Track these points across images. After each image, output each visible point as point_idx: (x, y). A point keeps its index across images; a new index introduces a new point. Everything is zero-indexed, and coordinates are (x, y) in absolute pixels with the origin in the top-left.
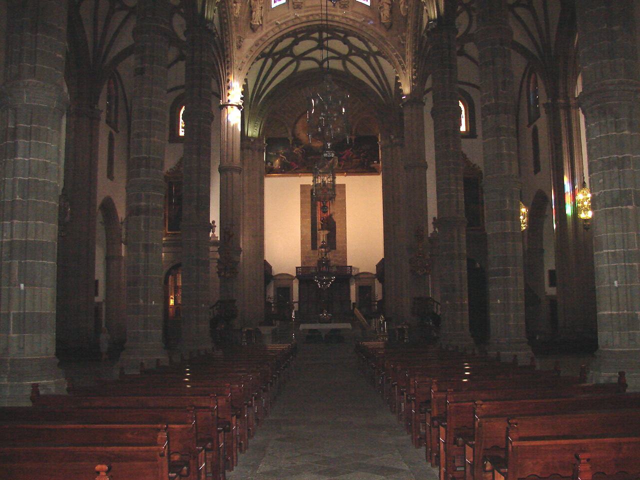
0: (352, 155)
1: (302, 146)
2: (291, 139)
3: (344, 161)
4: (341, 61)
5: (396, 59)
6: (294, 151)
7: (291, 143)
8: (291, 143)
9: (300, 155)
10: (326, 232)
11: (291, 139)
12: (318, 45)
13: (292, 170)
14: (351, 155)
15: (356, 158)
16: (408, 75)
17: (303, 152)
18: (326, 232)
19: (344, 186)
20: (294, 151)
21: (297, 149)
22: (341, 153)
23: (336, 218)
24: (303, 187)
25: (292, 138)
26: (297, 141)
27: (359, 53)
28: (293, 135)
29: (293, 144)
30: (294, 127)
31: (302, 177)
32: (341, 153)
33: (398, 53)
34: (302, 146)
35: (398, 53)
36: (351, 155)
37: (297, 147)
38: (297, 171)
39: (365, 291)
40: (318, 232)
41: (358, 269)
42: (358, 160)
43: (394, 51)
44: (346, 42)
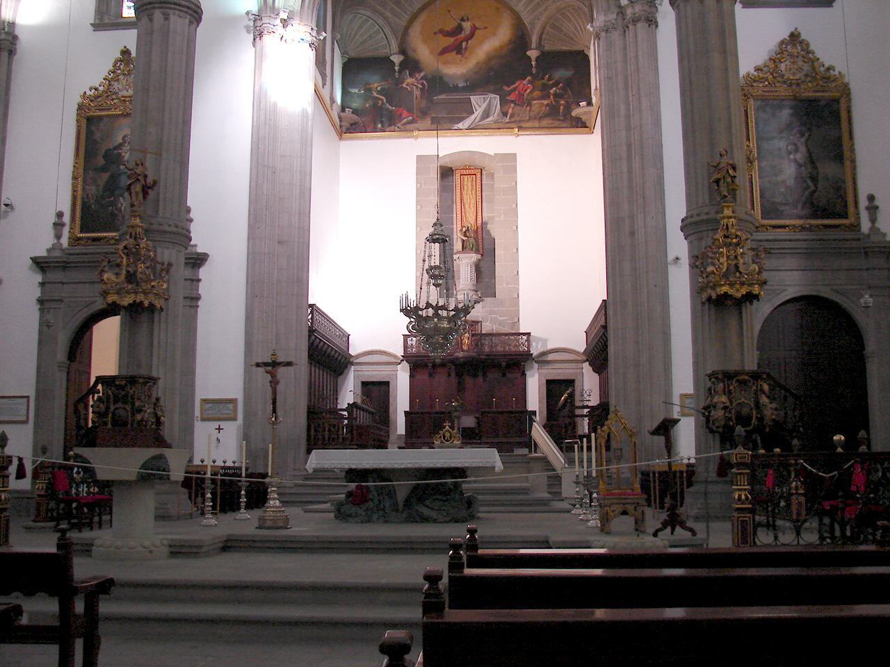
1: (422, 74)
2: (397, 59)
6: (404, 85)
7: (397, 68)
8: (397, 68)
9: (417, 93)
10: (474, 257)
11: (397, 59)
13: (399, 125)
14: (528, 91)
15: (542, 98)
18: (474, 257)
19: (512, 157)
20: (404, 85)
21: (410, 80)
23: (496, 230)
26: (411, 65)
28: (403, 52)
29: (400, 72)
31: (420, 140)
32: (506, 88)
34: (422, 74)
36: (528, 91)
37: (411, 75)
38: (408, 127)
39: (557, 389)
40: (455, 257)
41: (545, 341)
42: (545, 102)
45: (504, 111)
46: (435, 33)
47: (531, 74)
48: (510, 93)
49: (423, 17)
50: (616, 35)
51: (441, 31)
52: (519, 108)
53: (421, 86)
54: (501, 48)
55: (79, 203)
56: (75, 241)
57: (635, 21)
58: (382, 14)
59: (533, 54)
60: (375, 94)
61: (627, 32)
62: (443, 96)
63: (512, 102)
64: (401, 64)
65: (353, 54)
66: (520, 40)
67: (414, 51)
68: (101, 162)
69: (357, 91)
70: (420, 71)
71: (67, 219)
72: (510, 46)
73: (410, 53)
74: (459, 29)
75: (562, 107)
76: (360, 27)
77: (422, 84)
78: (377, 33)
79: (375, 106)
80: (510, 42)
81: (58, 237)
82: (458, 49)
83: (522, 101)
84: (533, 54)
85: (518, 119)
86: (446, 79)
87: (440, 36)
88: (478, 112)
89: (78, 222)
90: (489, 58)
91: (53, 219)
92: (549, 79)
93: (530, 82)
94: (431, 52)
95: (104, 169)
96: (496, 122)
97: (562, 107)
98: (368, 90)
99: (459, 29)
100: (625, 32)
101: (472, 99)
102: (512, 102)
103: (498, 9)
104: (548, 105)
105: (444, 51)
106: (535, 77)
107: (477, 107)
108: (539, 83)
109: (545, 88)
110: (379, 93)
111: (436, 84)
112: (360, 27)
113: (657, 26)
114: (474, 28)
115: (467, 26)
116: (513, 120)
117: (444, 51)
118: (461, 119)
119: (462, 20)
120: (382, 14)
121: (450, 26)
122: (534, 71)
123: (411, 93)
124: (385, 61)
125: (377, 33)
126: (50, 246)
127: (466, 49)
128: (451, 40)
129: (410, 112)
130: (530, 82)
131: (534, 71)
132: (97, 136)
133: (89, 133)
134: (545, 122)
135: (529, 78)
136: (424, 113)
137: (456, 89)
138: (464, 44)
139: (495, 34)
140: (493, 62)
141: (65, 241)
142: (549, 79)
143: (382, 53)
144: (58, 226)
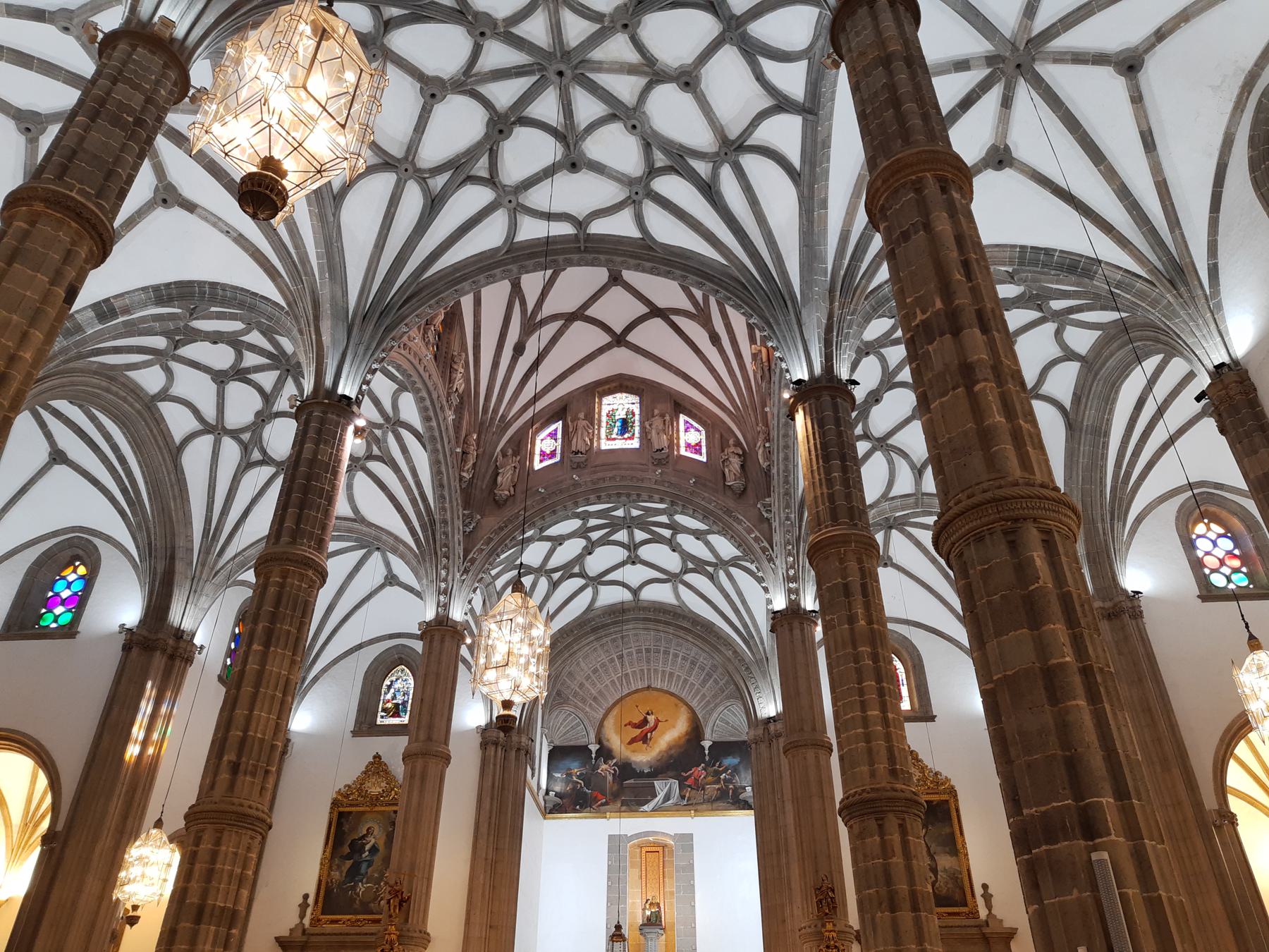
1: (614, 761)
2: (594, 748)
4: (668, 586)
5: (756, 545)
6: (599, 771)
7: (593, 756)
8: (593, 756)
9: (610, 778)
11: (594, 748)
12: (629, 557)
16: (780, 569)
17: (614, 770)
19: (690, 837)
20: (599, 771)
21: (604, 767)
24: (616, 843)
26: (605, 753)
27: (699, 566)
28: (599, 742)
29: (596, 759)
30: (601, 725)
33: (758, 535)
34: (614, 761)
35: (758, 535)
42: (717, 786)
43: (749, 532)
44: (675, 547)
45: (683, 794)
46: (625, 725)
47: (704, 762)
49: (615, 712)
51: (630, 724)
52: (694, 792)
53: (613, 772)
54: (679, 738)
55: (323, 887)
56: (315, 921)
58: (582, 710)
59: (707, 744)
60: (575, 779)
62: (632, 781)
63: (689, 786)
64: (597, 751)
65: (557, 743)
66: (696, 732)
67: (608, 740)
68: (346, 850)
69: (559, 775)
70: (614, 758)
71: (311, 901)
72: (687, 737)
73: (605, 743)
74: (645, 721)
75: (731, 791)
76: (564, 720)
77: (614, 770)
78: (578, 725)
79: (574, 789)
80: (687, 733)
81: (302, 916)
82: (644, 739)
83: (699, 787)
84: (707, 744)
85: (694, 802)
86: (634, 766)
87: (629, 727)
88: (660, 796)
89: (320, 904)
90: (670, 748)
91: (300, 900)
92: (719, 767)
93: (704, 769)
95: (348, 857)
97: (731, 791)
98: (569, 775)
99: (645, 721)
101: (656, 784)
102: (689, 786)
103: (676, 705)
104: (719, 789)
105: (633, 741)
106: (708, 765)
107: (660, 791)
108: (710, 769)
109: (717, 773)
110: (578, 777)
111: (626, 770)
112: (564, 720)
114: (657, 721)
115: (651, 719)
116: (690, 802)
117: (633, 741)
118: (647, 802)
119: (648, 714)
120: (582, 710)
122: (707, 758)
123: (605, 778)
124: (584, 750)
125: (578, 725)
126: (293, 926)
127: (650, 739)
129: (605, 795)
130: (704, 769)
131: (707, 758)
132: (346, 828)
133: (339, 825)
134: (715, 805)
135: (703, 765)
136: (615, 796)
137: (641, 775)
138: (649, 734)
139: (674, 727)
140: (673, 752)
141: (307, 921)
142: (719, 767)
143: (582, 742)
144: (304, 906)
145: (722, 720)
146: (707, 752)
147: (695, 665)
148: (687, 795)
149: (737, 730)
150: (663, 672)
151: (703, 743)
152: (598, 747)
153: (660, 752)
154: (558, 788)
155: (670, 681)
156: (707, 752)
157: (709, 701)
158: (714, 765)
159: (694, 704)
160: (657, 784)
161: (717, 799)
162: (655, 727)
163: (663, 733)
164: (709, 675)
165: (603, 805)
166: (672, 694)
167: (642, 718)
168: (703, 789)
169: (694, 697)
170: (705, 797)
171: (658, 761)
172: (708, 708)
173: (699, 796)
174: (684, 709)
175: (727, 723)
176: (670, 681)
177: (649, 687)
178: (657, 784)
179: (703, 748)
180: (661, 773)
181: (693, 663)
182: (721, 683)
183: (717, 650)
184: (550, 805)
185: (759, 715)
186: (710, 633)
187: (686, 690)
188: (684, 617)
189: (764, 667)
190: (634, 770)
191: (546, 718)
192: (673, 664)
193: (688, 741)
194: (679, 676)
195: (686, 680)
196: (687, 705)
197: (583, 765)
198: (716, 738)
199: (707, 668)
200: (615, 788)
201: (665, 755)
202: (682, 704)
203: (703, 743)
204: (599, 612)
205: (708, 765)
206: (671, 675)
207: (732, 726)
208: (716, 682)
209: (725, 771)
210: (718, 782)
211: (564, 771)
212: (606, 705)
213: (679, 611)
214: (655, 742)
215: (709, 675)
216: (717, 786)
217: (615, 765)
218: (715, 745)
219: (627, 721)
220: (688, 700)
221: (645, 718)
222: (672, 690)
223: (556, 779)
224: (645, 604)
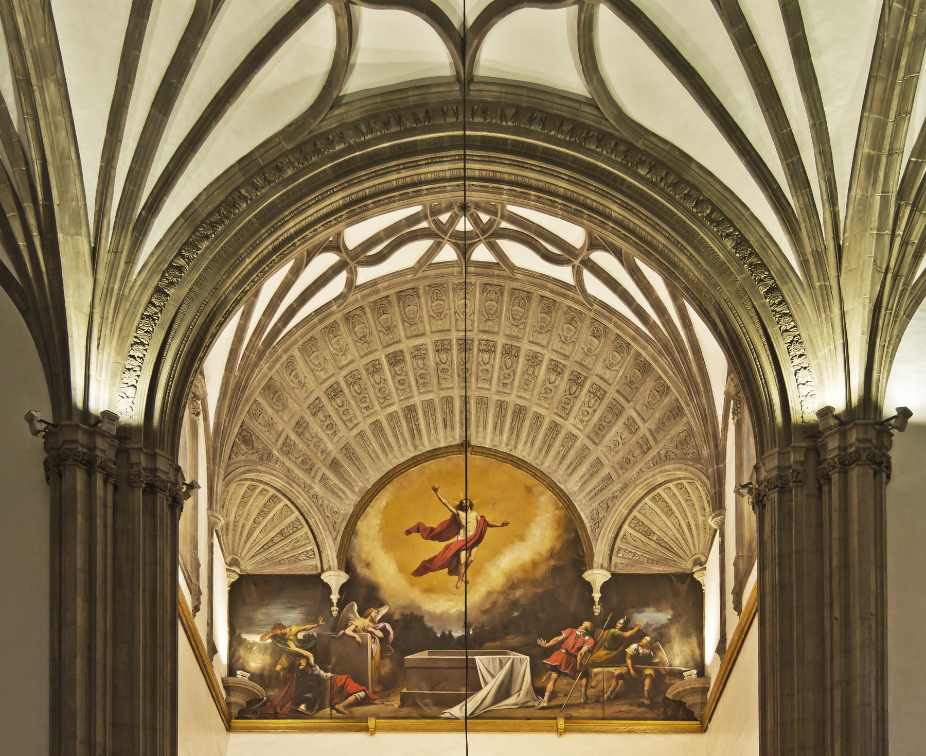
0: (590, 651)
1: (384, 611)
2: (335, 579)
3: (554, 675)
6: (349, 631)
7: (335, 597)
8: (335, 597)
9: (374, 647)
14: (585, 648)
17: (384, 630)
20: (349, 631)
22: (542, 643)
25: (344, 578)
28: (347, 565)
29: (341, 604)
30: (350, 531)
32: (542, 643)
34: (384, 611)
36: (585, 648)
37: (362, 613)
45: (539, 684)
47: (590, 617)
48: (549, 652)
49: (382, 500)
50: (799, 498)
51: (418, 529)
52: (564, 681)
53: (380, 634)
54: (535, 564)
57: (845, 464)
59: (597, 577)
60: (293, 647)
61: (825, 489)
62: (424, 655)
63: (555, 669)
64: (343, 589)
65: (249, 567)
67: (368, 565)
70: (382, 604)
73: (361, 570)
77: (384, 630)
78: (295, 527)
79: (292, 668)
80: (552, 554)
84: (597, 577)
86: (428, 623)
90: (512, 585)
92: (625, 628)
93: (589, 632)
94: (401, 568)
96: (524, 706)
98: (280, 639)
100: (820, 489)
103: (529, 489)
105: (425, 568)
106: (598, 623)
108: (604, 634)
110: (302, 643)
113: (888, 477)
114: (483, 525)
116: (554, 703)
117: (425, 568)
120: (307, 488)
121: (437, 519)
122: (597, 610)
123: (363, 646)
125: (295, 527)
127: (467, 565)
128: (443, 545)
129: (360, 679)
131: (597, 610)
135: (587, 624)
137: (446, 642)
138: (463, 554)
139: (521, 538)
140: (518, 593)
142: (625, 628)
143: (307, 566)
145: (639, 525)
146: (597, 596)
147: (581, 386)
148: (550, 687)
149: (670, 549)
150: (501, 405)
151: (588, 576)
152: (344, 578)
153: (489, 594)
154: (256, 661)
155: (516, 430)
156: (597, 596)
157: (609, 478)
158: (612, 625)
159: (571, 486)
160: (482, 662)
161: (617, 697)
162: (479, 538)
163: (497, 552)
164: (615, 411)
165: (358, 703)
166: (519, 464)
167: (447, 516)
168: (587, 675)
169: (572, 469)
170: (590, 692)
171: (485, 612)
172: (607, 494)
173: (576, 688)
174: (546, 499)
175: (648, 533)
176: (516, 430)
177: (465, 445)
178: (482, 662)
179: (588, 587)
180: (493, 639)
181: (577, 380)
182: (644, 429)
183: (690, 236)
184: (239, 699)
185: (795, 417)
186: (674, 185)
187: (552, 453)
188: (603, 138)
189: (825, 276)
190: (429, 631)
191: (219, 486)
192: (526, 385)
193: (556, 571)
194: (538, 417)
195: (555, 428)
196: (552, 487)
197: (311, 617)
198: (622, 564)
199: (612, 392)
200: (387, 668)
201: (501, 599)
202: (540, 488)
203: (588, 576)
204: (355, 115)
205: (598, 623)
206: (520, 412)
207: (659, 542)
208: (631, 427)
209: (638, 636)
210: (619, 660)
211: (269, 629)
212: (364, 483)
213: (588, 117)
214: (478, 572)
215: (615, 411)
216: (617, 671)
217: (386, 618)
218: (617, 582)
219: (412, 524)
220: (558, 477)
221: (455, 517)
222: (521, 452)
223: (250, 647)
224: (490, 95)
